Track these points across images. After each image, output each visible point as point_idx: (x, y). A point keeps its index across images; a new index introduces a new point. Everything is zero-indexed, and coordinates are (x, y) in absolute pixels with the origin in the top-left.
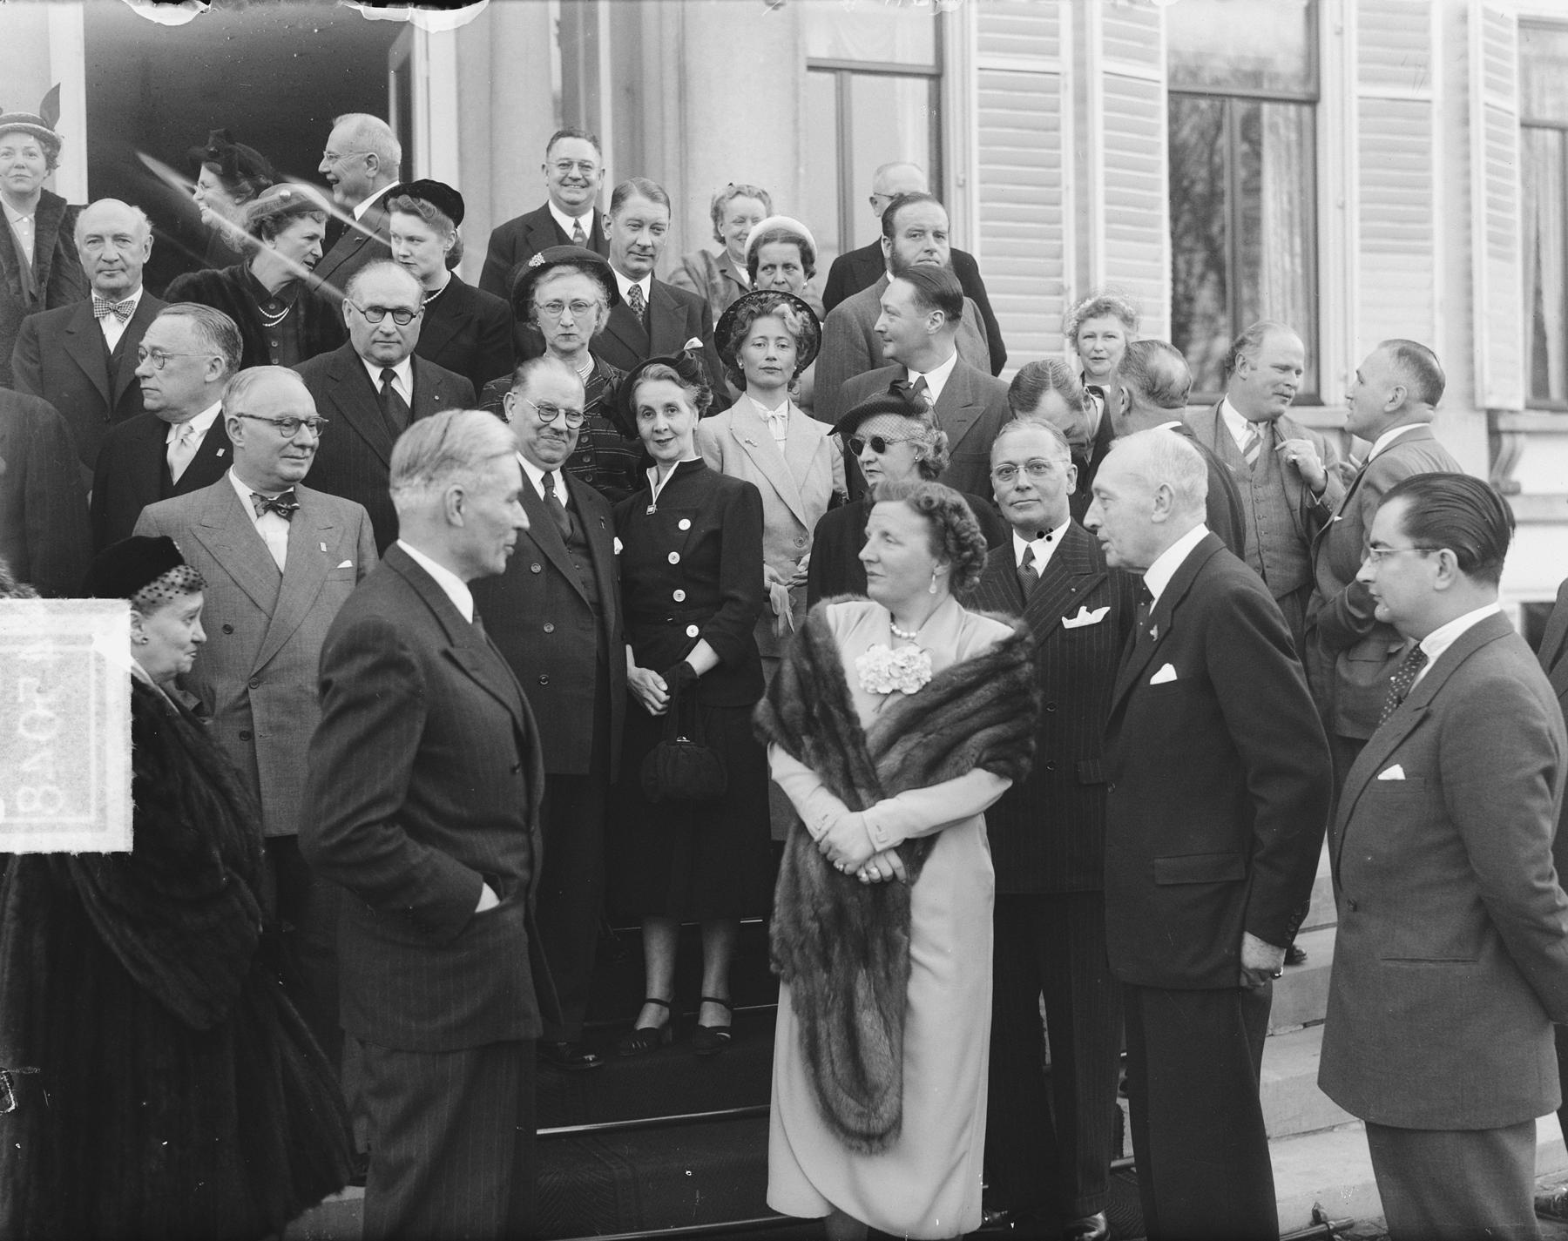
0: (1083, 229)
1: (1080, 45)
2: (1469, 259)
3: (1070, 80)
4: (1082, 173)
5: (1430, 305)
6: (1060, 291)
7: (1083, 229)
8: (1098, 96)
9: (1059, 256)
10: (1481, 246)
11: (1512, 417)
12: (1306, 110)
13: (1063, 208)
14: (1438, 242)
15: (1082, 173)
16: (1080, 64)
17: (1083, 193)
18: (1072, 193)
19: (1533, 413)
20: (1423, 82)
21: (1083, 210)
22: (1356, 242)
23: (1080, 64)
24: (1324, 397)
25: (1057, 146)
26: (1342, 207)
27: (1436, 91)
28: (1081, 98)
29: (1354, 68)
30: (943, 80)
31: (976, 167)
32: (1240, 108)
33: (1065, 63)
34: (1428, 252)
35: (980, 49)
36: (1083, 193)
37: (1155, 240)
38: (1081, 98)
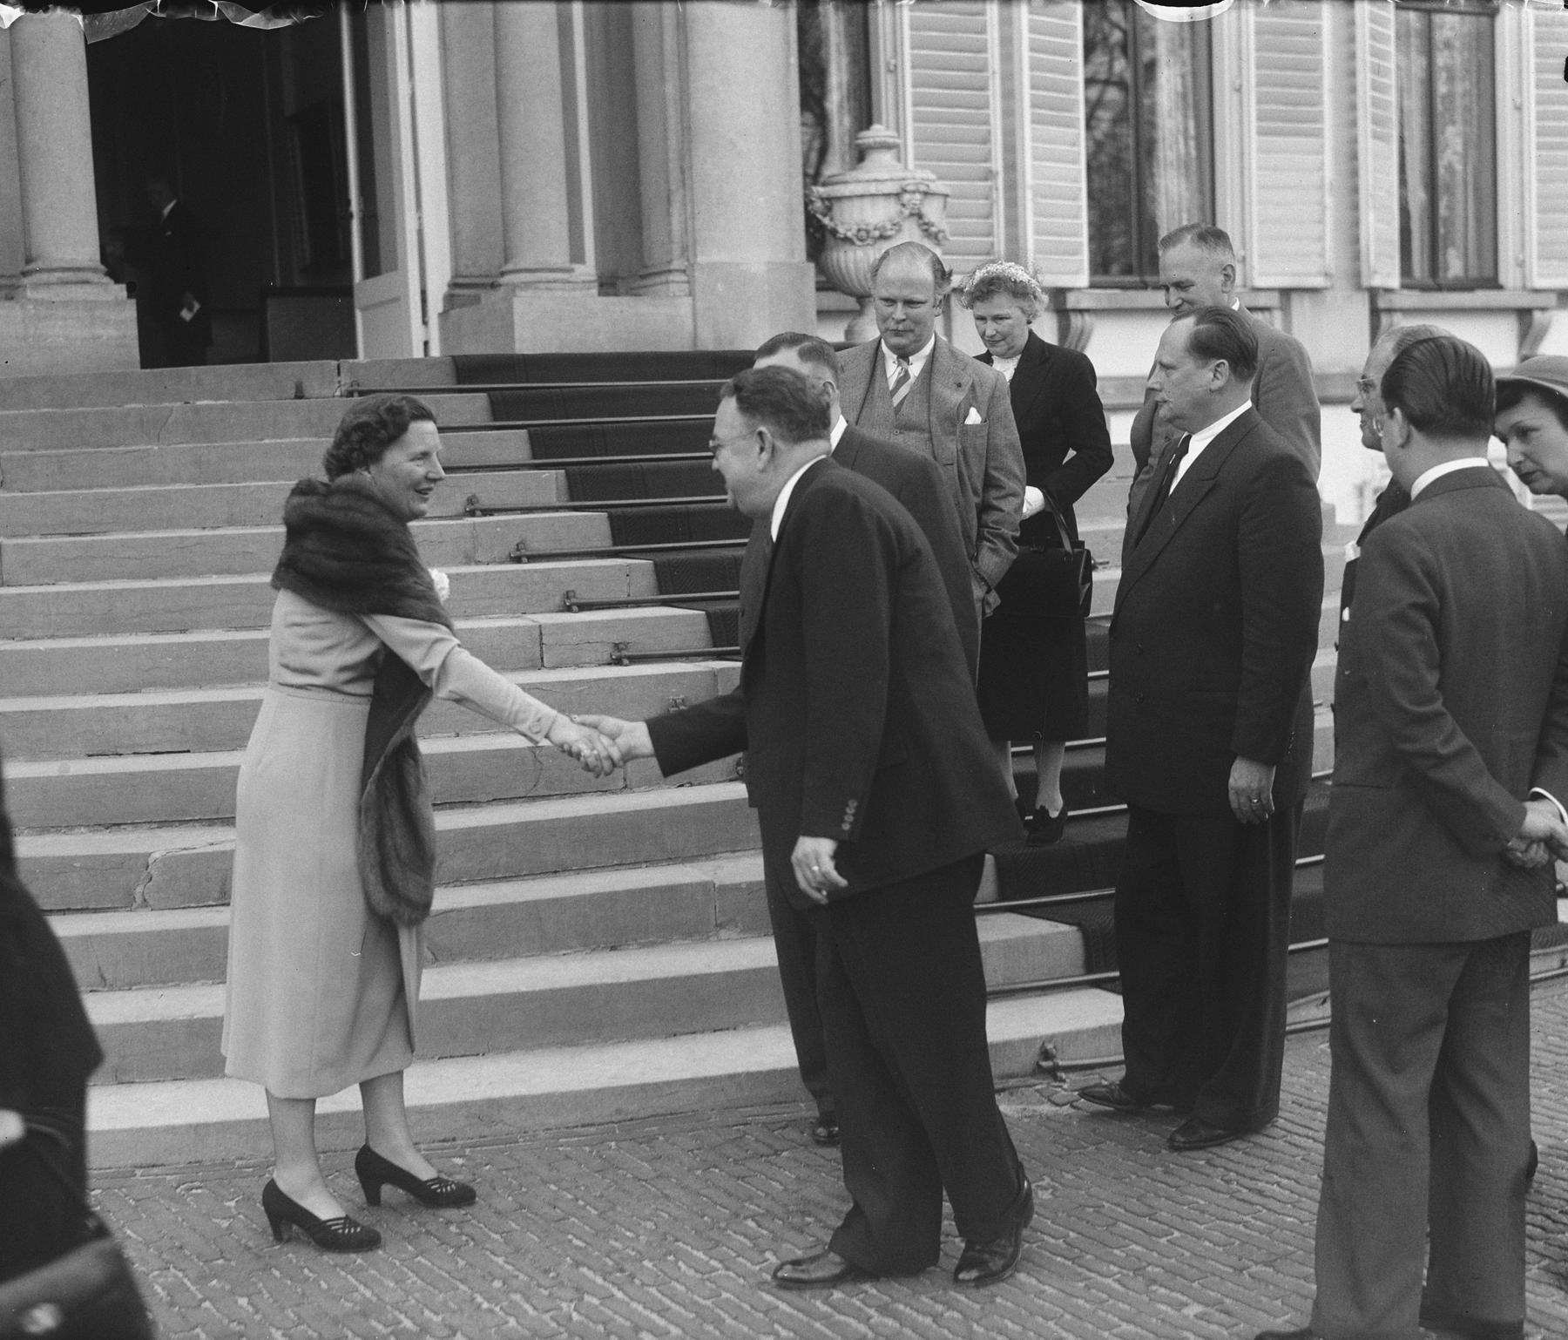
0: (1009, 113)
2: (1354, 141)
4: (1008, 57)
5: (1321, 187)
6: (989, 175)
7: (1009, 113)
9: (986, 140)
10: (1365, 127)
11: (1389, 296)
13: (990, 93)
14: (1328, 125)
15: (1008, 57)
17: (1008, 77)
18: (998, 76)
19: (1405, 292)
21: (1009, 95)
26: (1239, 90)
31: (907, 52)
34: (1319, 134)
36: (1008, 77)
37: (1070, 124)
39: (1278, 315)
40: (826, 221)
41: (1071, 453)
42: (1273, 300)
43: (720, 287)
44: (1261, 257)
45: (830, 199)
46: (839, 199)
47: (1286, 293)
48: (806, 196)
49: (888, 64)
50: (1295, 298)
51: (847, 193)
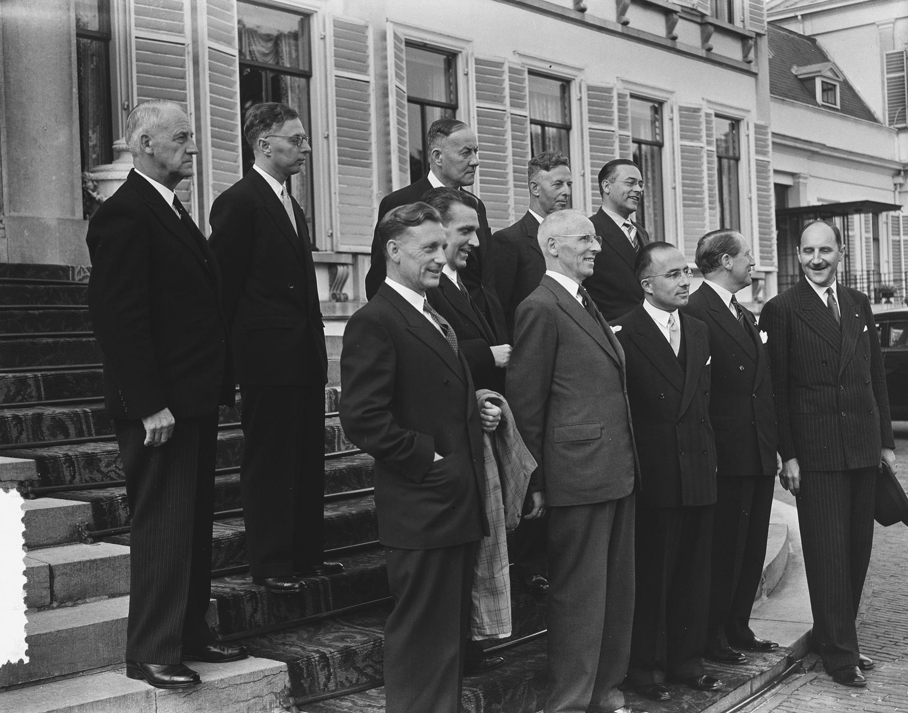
1: (195, 31)
3: (190, 48)
8: (205, 61)
12: (303, 81)
16: (195, 42)
20: (364, 71)
22: (334, 158)
23: (195, 42)
24: (318, 246)
25: (184, 88)
27: (371, 77)
28: (196, 62)
29: (331, 61)
30: (111, 43)
32: (270, 75)
33: (188, 40)
34: (368, 166)
35: (136, 26)
37: (234, 149)
38: (196, 62)
39: (351, 267)
40: (95, 194)
41: (708, 363)
42: (348, 259)
43: (26, 233)
44: (341, 233)
45: (97, 181)
46: (103, 180)
47: (355, 255)
48: (83, 178)
49: (123, 105)
50: (360, 257)
51: (109, 178)
